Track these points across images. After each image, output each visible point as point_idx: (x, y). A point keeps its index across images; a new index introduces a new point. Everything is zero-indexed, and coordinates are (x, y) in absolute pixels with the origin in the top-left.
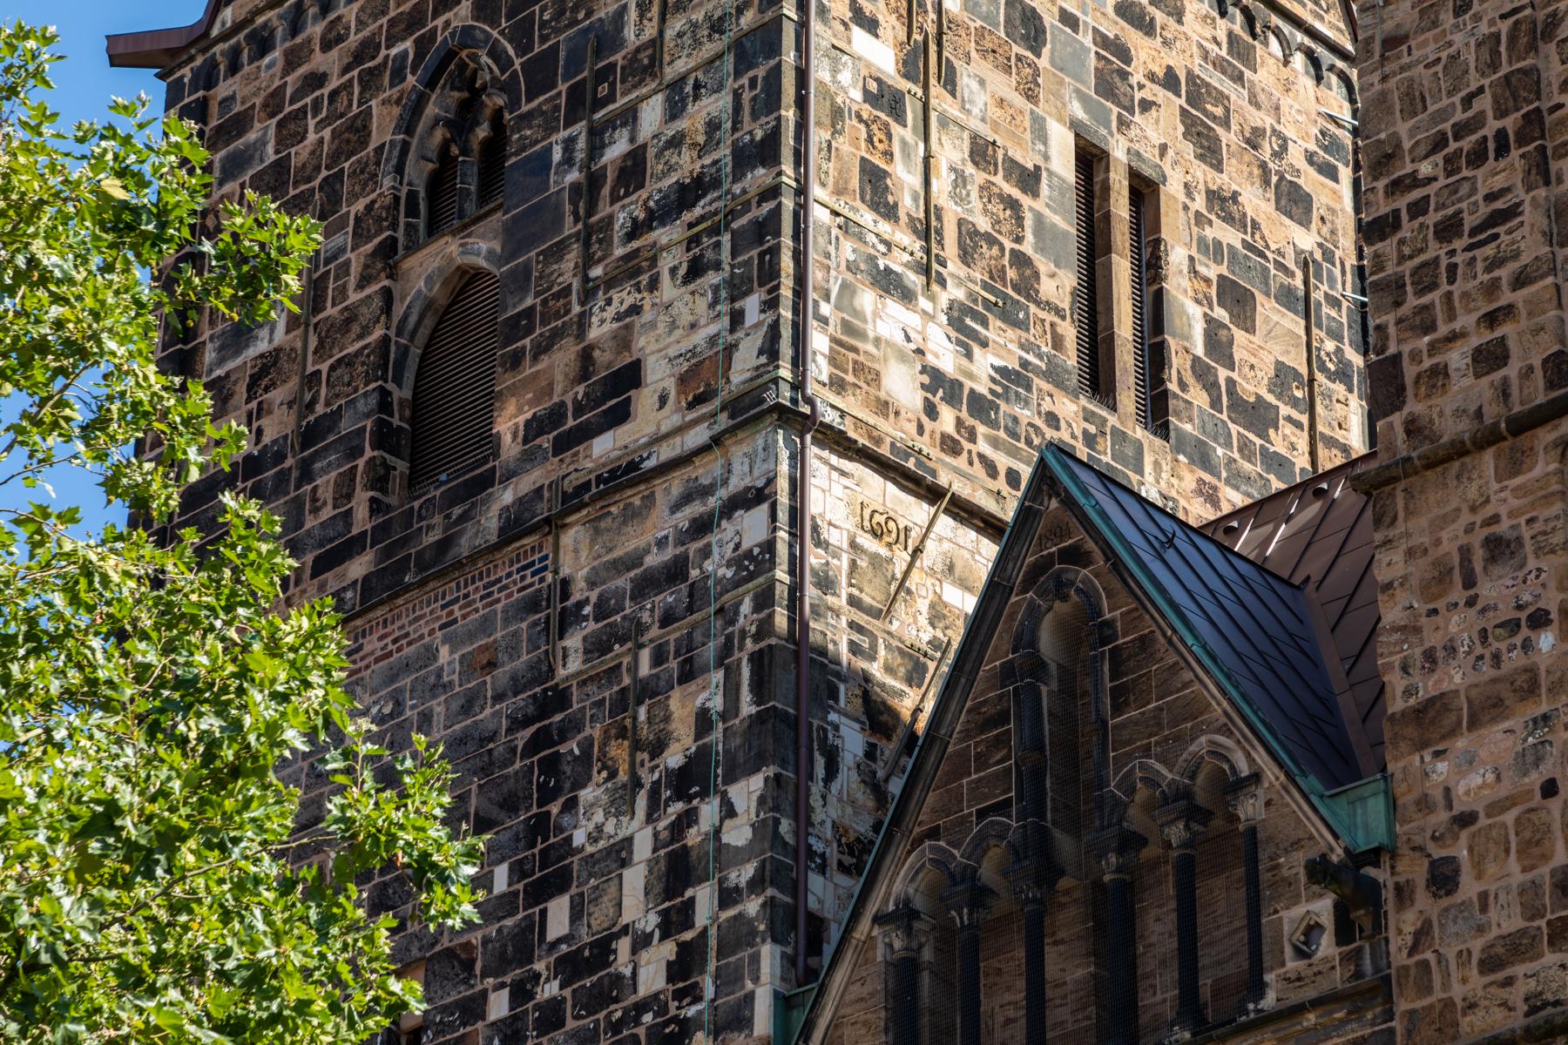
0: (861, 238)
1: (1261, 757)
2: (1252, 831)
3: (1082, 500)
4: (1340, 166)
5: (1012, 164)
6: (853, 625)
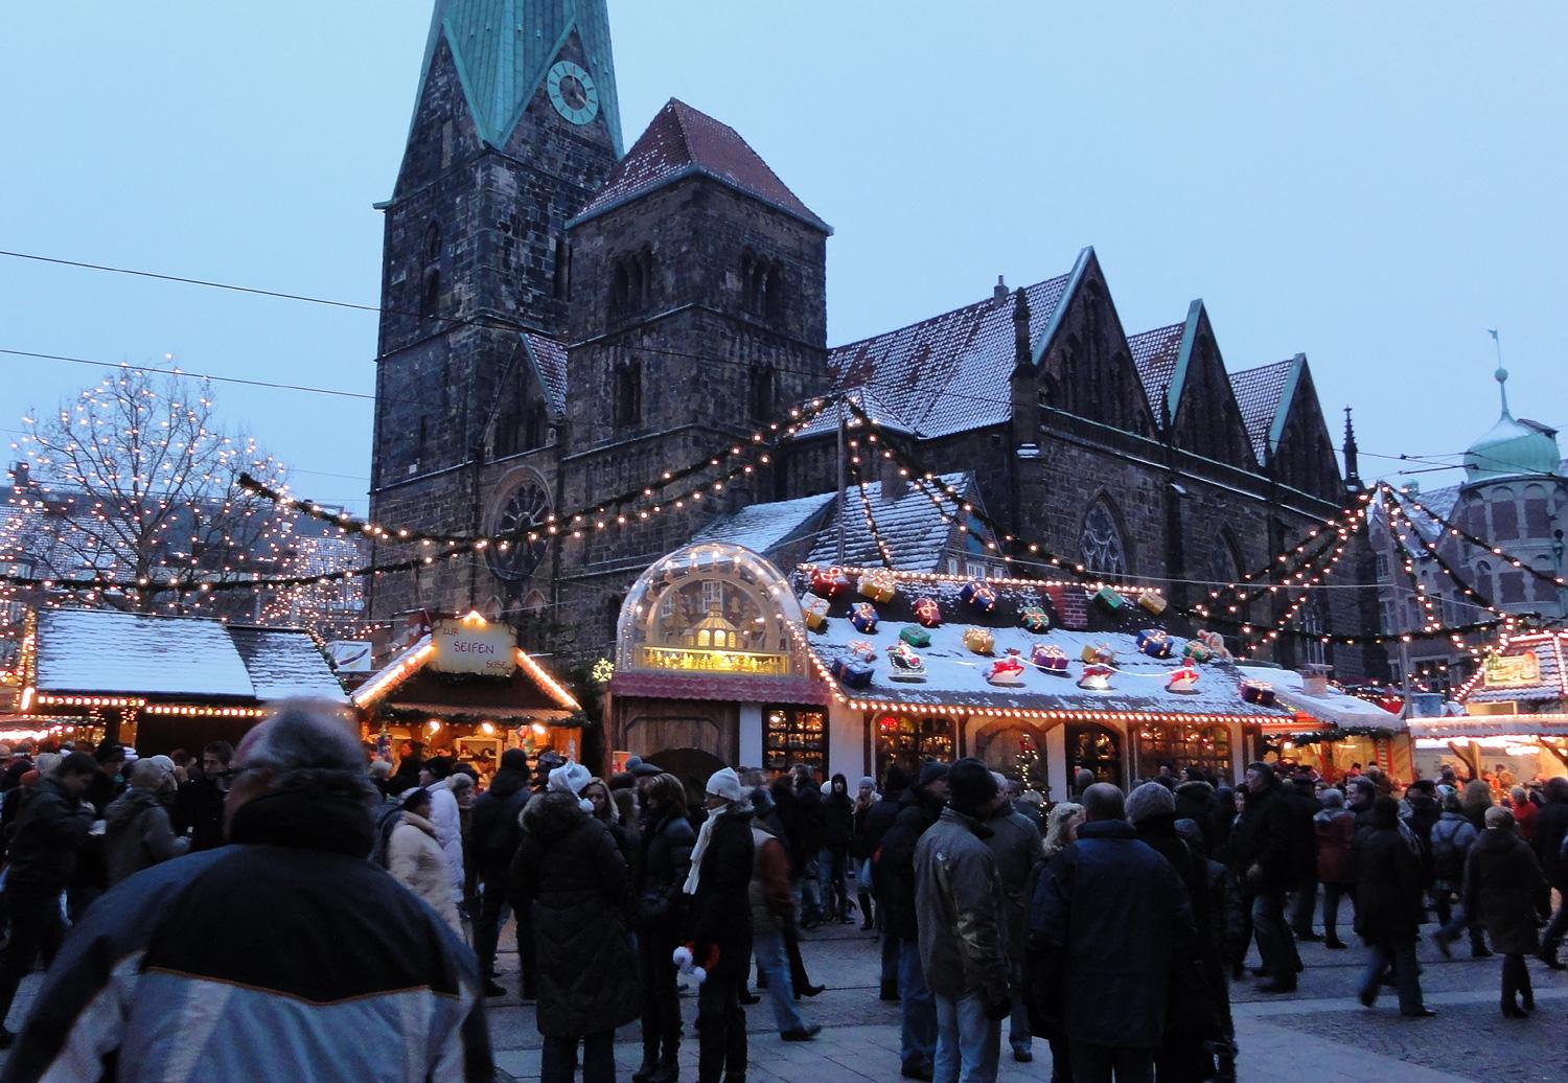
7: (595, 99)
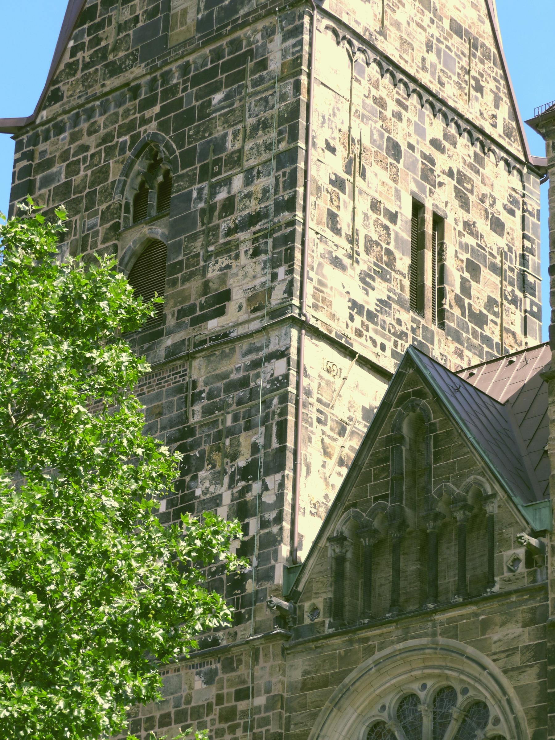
0: (326, 243)
1: (497, 487)
2: (492, 517)
3: (425, 371)
4: (516, 210)
5: (387, 211)
6: (319, 411)
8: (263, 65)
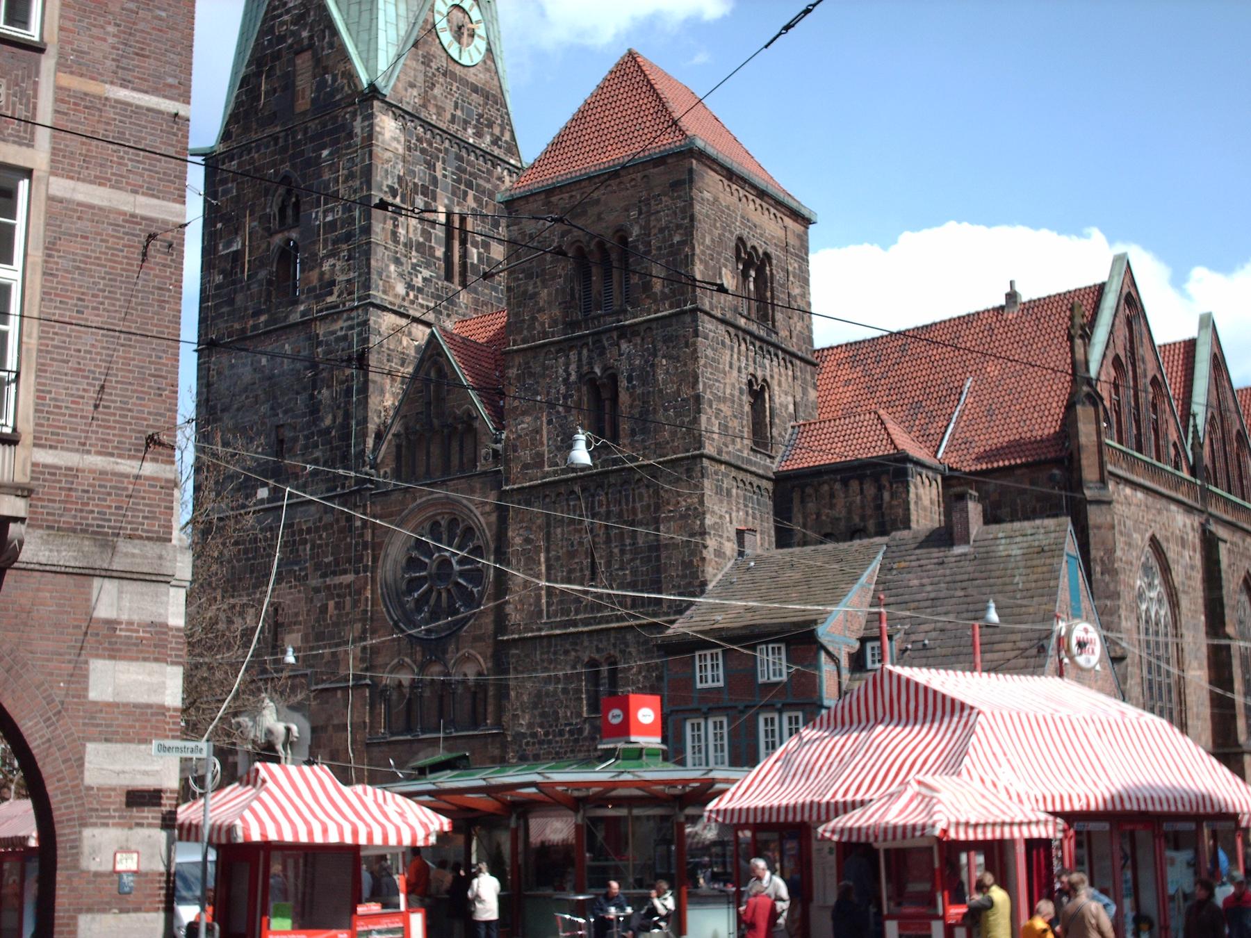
7: (483, 34)
8: (351, 135)
